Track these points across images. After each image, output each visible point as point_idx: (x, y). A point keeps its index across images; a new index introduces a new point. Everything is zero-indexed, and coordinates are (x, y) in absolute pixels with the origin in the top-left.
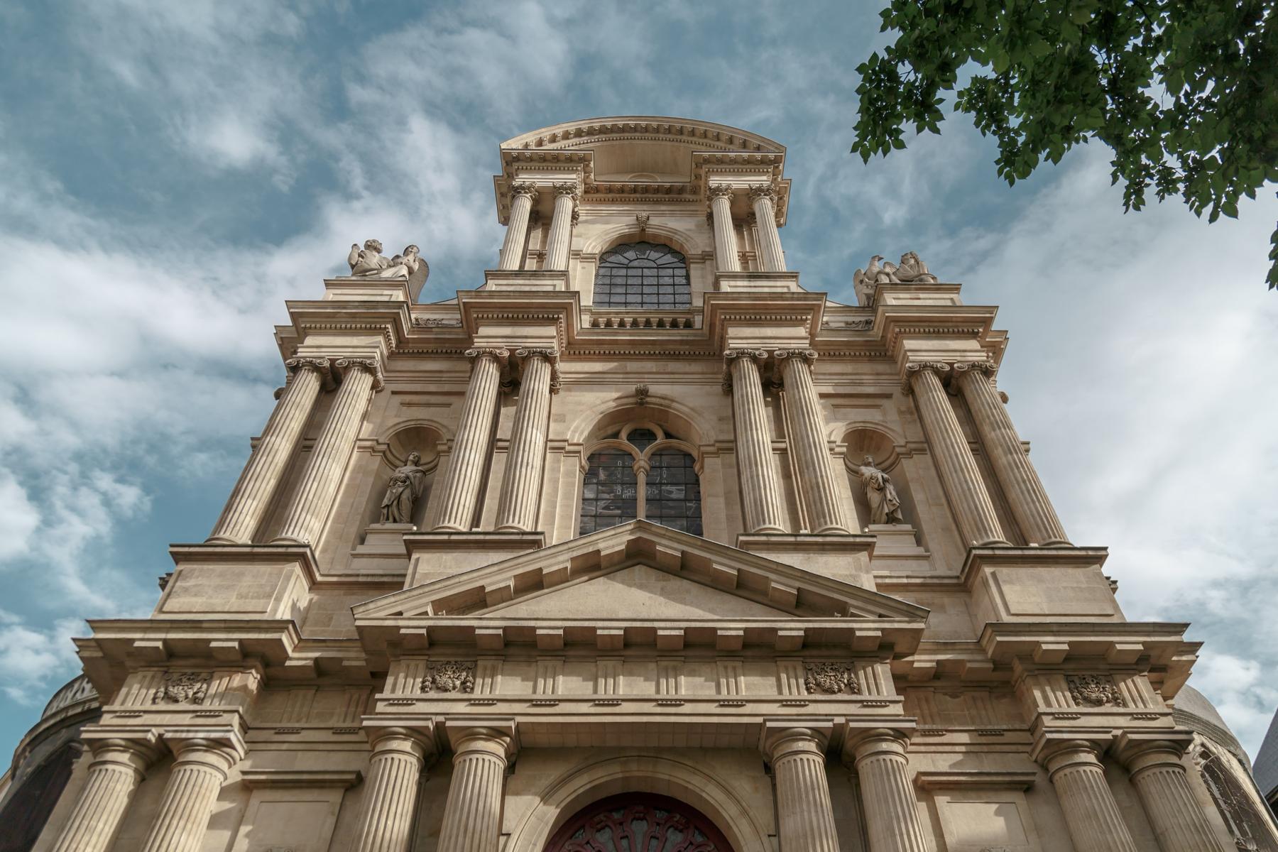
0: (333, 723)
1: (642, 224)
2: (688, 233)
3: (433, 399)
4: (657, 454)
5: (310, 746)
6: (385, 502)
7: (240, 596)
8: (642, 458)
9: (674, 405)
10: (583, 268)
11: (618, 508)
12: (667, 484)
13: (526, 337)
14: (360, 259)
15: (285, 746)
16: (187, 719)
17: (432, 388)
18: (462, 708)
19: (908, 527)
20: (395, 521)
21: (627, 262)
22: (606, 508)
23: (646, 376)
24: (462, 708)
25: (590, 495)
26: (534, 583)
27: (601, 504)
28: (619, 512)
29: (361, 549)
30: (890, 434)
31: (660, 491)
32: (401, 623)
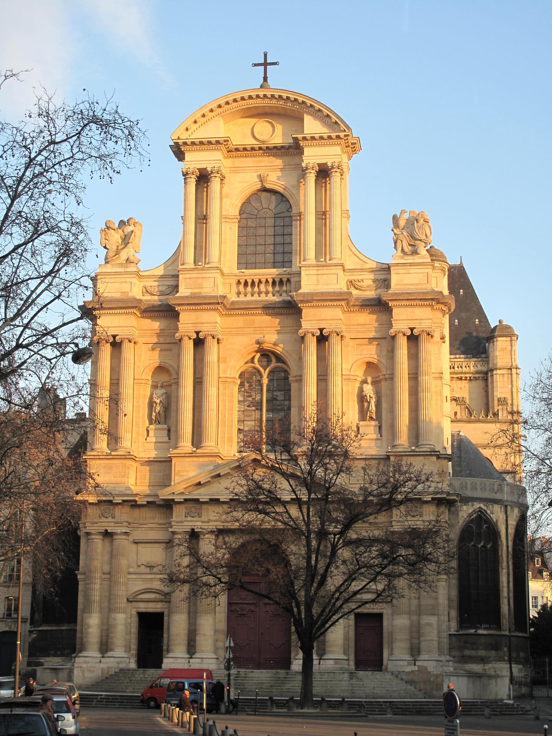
2: (291, 189)
5: (151, 529)
7: (114, 477)
10: (230, 228)
11: (254, 406)
12: (276, 391)
13: (203, 323)
15: (144, 529)
16: (112, 524)
18: (199, 524)
20: (159, 423)
22: (249, 406)
23: (265, 329)
24: (199, 524)
25: (241, 399)
27: (246, 404)
28: (254, 408)
31: (273, 395)
32: (174, 497)
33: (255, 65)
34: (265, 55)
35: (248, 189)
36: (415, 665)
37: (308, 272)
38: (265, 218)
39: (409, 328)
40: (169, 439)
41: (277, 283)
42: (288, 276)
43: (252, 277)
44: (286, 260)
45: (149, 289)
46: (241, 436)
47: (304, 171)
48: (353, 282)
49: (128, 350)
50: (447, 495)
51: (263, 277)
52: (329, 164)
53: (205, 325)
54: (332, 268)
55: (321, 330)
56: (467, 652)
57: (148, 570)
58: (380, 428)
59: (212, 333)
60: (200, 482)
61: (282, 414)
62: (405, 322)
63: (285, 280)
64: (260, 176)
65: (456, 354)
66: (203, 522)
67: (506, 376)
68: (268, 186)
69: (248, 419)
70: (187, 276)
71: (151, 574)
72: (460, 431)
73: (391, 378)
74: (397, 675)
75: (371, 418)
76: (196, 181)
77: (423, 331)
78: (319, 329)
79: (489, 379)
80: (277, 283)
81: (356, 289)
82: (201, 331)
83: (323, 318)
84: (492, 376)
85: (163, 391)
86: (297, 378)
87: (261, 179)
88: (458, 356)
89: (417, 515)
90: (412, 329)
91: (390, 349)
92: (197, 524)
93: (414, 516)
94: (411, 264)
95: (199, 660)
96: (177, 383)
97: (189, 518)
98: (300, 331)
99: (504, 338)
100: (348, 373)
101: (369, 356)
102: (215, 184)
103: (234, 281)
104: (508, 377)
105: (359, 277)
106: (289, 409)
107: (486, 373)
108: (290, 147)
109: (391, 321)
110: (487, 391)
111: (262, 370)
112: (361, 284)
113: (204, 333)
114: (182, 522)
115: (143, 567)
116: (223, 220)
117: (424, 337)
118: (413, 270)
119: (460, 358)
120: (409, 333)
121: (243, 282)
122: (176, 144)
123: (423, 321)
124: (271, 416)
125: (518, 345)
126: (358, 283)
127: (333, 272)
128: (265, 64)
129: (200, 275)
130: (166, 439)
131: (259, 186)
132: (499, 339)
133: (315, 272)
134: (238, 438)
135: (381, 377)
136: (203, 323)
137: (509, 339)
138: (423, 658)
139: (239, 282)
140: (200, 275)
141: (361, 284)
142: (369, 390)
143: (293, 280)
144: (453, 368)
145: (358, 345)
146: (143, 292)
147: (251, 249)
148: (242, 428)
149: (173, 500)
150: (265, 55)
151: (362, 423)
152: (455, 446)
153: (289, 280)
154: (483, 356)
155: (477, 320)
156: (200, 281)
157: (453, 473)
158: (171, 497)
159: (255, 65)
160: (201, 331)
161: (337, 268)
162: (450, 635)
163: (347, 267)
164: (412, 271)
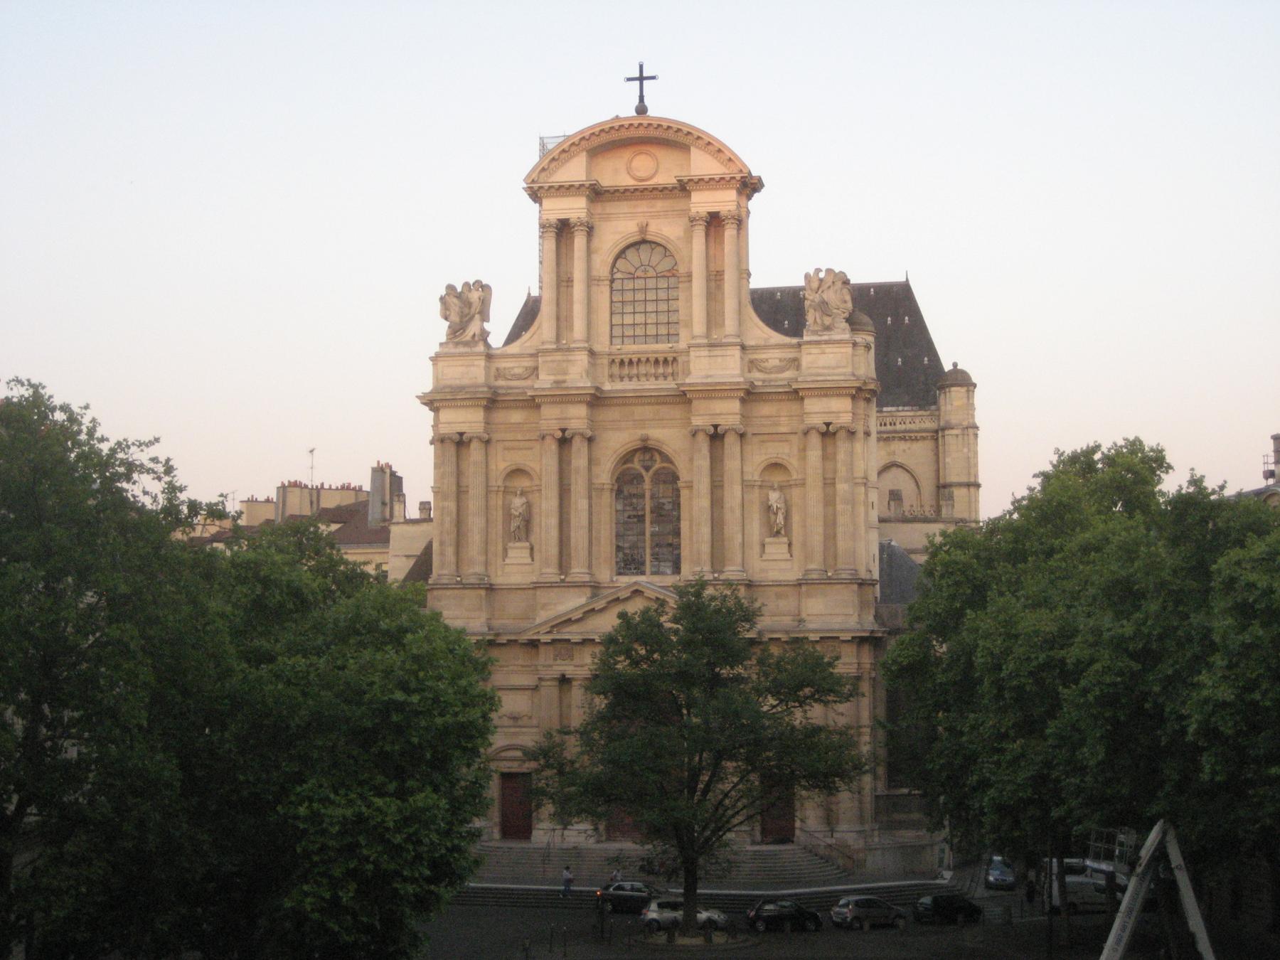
0: (520, 662)
1: (643, 229)
3: (522, 444)
4: (657, 473)
6: (512, 529)
8: (647, 477)
9: (664, 446)
13: (570, 419)
14: (448, 313)
17: (519, 437)
18: (571, 668)
19: (785, 540)
21: (633, 270)
27: (626, 514)
28: (635, 520)
29: (508, 561)
30: (790, 468)
33: (629, 79)
34: (641, 67)
36: (832, 836)
37: (698, 353)
38: (645, 278)
39: (825, 423)
40: (533, 560)
41: (661, 363)
42: (675, 355)
43: (629, 356)
44: (672, 332)
46: (621, 555)
53: (573, 421)
54: (730, 348)
55: (716, 427)
56: (897, 816)
57: (511, 723)
58: (790, 545)
59: (581, 431)
61: (670, 527)
62: (819, 415)
63: (670, 359)
65: (898, 406)
66: (576, 666)
67: (960, 437)
68: (649, 238)
69: (629, 533)
70: (549, 358)
71: (515, 727)
72: (891, 540)
74: (811, 851)
76: (557, 233)
77: (841, 428)
79: (940, 439)
80: (661, 363)
81: (760, 371)
83: (718, 412)
84: (943, 436)
85: (524, 500)
86: (688, 484)
88: (900, 408)
90: (828, 424)
91: (801, 447)
92: (569, 670)
94: (827, 342)
95: (575, 833)
97: (559, 662)
99: (959, 388)
101: (775, 455)
104: (963, 439)
105: (763, 356)
106: (679, 519)
107: (937, 432)
108: (674, 188)
110: (937, 455)
111: (644, 472)
112: (766, 364)
113: (572, 431)
114: (550, 666)
115: (505, 718)
117: (842, 434)
118: (829, 349)
119: (903, 411)
123: (841, 415)
124: (657, 529)
125: (979, 396)
126: (763, 365)
127: (729, 353)
128: (641, 79)
129: (565, 358)
130: (529, 560)
131: (637, 238)
132: (953, 389)
133: (706, 353)
134: (617, 557)
135: (792, 483)
136: (570, 419)
137: (965, 389)
138: (841, 829)
140: (565, 358)
141: (766, 364)
143: (680, 359)
144: (895, 424)
148: (620, 544)
149: (539, 640)
150: (641, 67)
151: (768, 540)
152: (885, 560)
153: (675, 359)
154: (933, 407)
155: (926, 359)
156: (565, 365)
157: (881, 596)
158: (535, 637)
159: (629, 79)
161: (734, 348)
162: (877, 797)
164: (828, 350)
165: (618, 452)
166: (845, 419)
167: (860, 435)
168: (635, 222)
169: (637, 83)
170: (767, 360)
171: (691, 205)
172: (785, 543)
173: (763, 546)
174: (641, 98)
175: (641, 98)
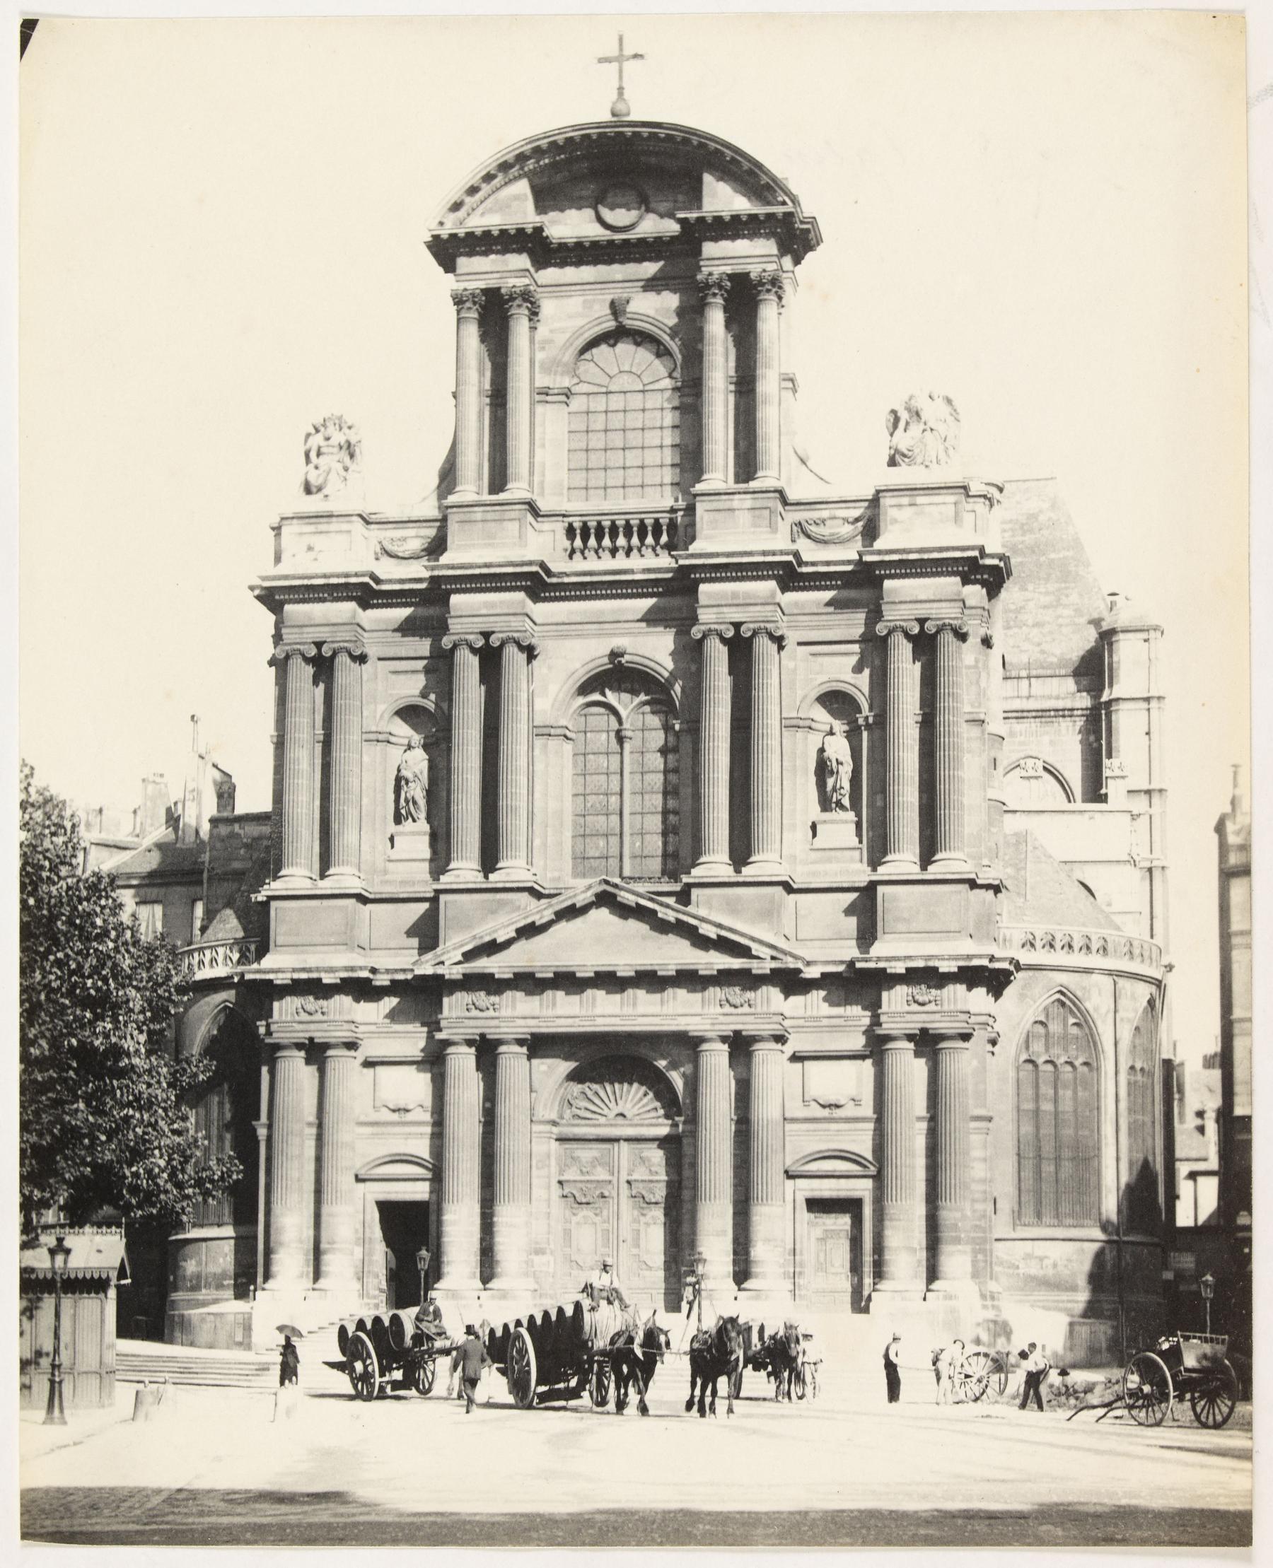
26: (530, 931)
35: (590, 329)
45: (389, 547)
47: (701, 290)
48: (804, 524)
49: (345, 670)
50: (991, 961)
51: (623, 517)
52: (753, 276)
60: (495, 940)
64: (613, 304)
73: (881, 723)
75: (842, 807)
77: (944, 625)
78: (733, 624)
82: (493, 632)
87: (616, 309)
89: (930, 1002)
93: (923, 1004)
96: (448, 739)
98: (694, 630)
100: (794, 715)
102: (520, 327)
103: (560, 527)
109: (880, 606)
116: (538, 398)
117: (948, 637)
120: (916, 630)
121: (577, 525)
122: (436, 238)
139: (570, 532)
142: (839, 749)
145: (813, 655)
146: (376, 554)
147: (596, 459)
160: (493, 632)
163: (792, 496)
165: (576, 676)
166: (948, 612)
167: (974, 641)
168: (609, 298)
169: (615, 53)
170: (823, 521)
171: (702, 263)
172: (846, 822)
173: (814, 827)
174: (621, 90)
175: (621, 90)
